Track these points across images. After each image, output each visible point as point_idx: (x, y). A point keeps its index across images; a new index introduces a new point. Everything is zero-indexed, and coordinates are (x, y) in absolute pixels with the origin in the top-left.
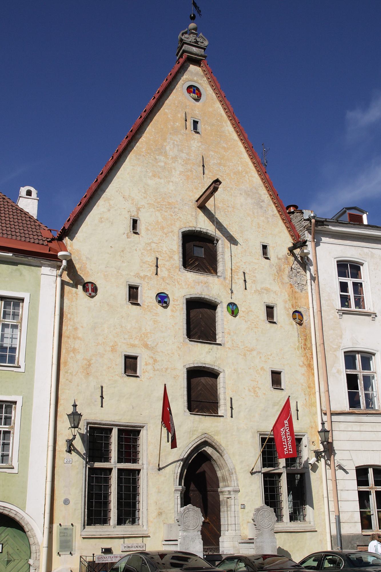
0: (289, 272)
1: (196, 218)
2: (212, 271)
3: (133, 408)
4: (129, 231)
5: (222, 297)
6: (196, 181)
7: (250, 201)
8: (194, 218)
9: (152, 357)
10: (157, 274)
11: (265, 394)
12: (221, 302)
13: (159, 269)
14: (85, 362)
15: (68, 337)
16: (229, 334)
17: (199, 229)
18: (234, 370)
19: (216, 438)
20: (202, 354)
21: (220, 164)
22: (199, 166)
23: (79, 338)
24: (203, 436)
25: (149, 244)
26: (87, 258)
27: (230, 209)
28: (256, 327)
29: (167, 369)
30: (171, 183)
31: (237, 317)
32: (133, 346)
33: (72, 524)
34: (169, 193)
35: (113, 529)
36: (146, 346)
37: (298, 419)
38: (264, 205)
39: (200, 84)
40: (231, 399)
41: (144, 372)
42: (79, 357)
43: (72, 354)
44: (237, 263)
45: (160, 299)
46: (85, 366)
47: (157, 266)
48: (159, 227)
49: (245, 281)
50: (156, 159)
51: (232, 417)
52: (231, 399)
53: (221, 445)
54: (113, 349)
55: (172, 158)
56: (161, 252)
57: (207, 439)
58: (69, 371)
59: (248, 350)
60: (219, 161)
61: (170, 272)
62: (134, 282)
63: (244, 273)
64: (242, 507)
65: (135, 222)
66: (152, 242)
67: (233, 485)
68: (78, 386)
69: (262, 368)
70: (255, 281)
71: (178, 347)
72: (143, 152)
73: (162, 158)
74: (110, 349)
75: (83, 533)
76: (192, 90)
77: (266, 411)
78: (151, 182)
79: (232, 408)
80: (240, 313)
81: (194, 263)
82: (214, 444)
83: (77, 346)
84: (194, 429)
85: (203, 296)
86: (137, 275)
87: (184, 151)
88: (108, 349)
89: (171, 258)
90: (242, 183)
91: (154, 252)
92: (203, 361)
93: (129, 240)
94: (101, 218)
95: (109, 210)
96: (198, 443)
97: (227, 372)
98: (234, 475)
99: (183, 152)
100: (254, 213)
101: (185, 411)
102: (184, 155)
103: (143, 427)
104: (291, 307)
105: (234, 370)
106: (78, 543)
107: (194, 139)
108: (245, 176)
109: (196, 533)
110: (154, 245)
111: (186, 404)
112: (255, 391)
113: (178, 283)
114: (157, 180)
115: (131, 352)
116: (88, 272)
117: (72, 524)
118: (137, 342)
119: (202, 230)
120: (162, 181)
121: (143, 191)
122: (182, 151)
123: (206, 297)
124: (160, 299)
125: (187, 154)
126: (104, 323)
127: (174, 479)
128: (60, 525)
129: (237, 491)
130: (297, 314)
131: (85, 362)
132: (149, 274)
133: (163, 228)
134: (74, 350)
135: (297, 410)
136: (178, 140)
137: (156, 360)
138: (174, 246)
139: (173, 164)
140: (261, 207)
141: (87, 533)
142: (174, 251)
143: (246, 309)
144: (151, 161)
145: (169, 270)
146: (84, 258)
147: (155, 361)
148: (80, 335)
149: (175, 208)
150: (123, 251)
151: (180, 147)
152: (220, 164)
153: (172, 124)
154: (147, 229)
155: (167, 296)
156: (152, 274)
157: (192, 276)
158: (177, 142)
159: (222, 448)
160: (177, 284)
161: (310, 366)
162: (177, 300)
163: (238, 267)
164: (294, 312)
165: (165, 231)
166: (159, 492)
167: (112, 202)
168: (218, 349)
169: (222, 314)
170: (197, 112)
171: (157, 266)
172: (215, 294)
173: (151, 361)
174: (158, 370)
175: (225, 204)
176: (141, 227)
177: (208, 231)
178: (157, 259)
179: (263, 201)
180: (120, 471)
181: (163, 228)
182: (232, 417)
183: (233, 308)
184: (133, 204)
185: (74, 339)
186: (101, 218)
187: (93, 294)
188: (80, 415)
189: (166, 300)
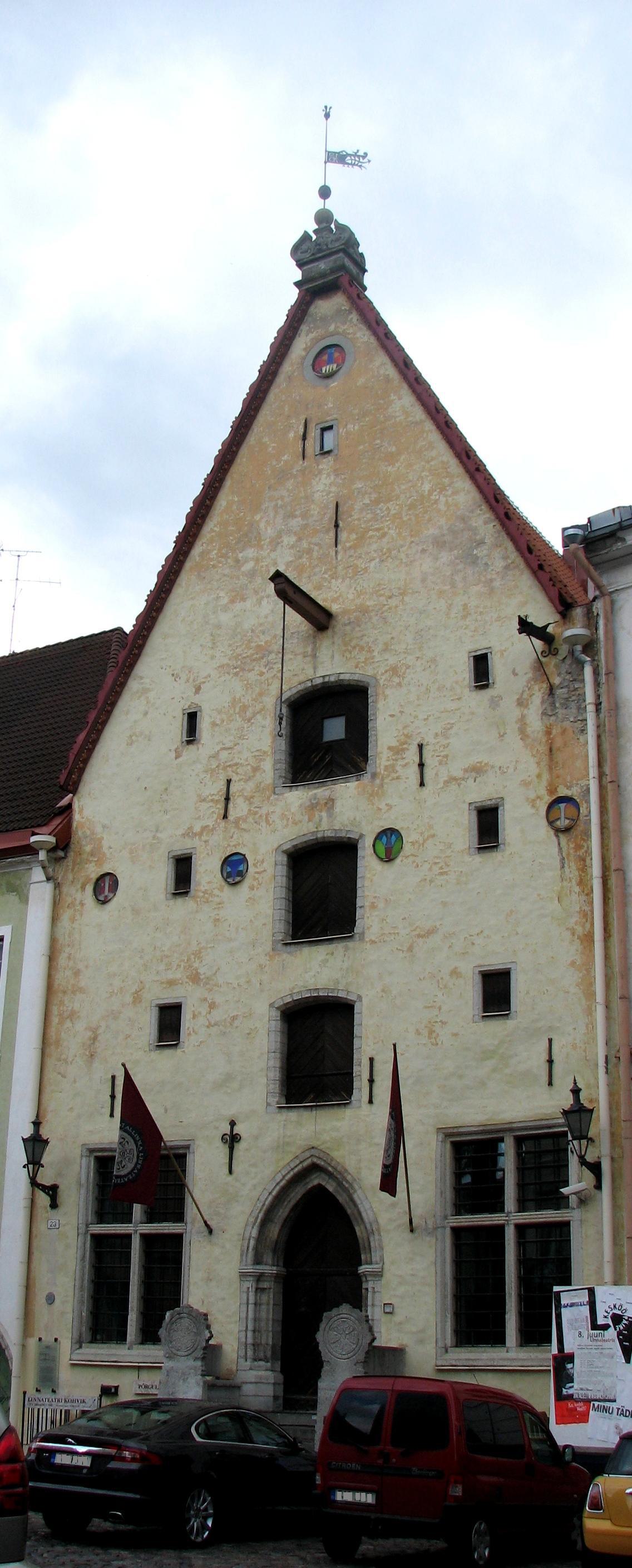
0: (543, 702)
1: (314, 656)
2: (353, 770)
3: (166, 1111)
4: (179, 743)
5: (363, 823)
6: (317, 570)
7: (445, 557)
8: (309, 659)
9: (205, 999)
10: (225, 817)
11: (456, 1035)
12: (362, 836)
13: (231, 805)
14: (89, 1034)
15: (65, 992)
16: (373, 906)
17: (319, 681)
18: (383, 991)
19: (335, 1154)
20: (316, 969)
21: (377, 502)
22: (327, 531)
23: (82, 990)
24: (308, 1154)
25: (215, 756)
26: (104, 827)
27: (393, 602)
28: (441, 874)
29: (234, 1018)
30: (264, 602)
31: (398, 861)
32: (171, 983)
33: (56, 1340)
34: (261, 625)
35: (127, 1352)
36: (195, 978)
37: (550, 1084)
38: (480, 552)
39: (332, 335)
40: (371, 1060)
41: (189, 1034)
42: (80, 1026)
43: (68, 1024)
44: (405, 727)
45: (229, 870)
46: (89, 1042)
47: (227, 799)
48: (237, 710)
49: (421, 765)
50: (237, 561)
51: (371, 1102)
52: (371, 1060)
53: (346, 1170)
54: (137, 998)
55: (271, 542)
56: (236, 764)
57: (315, 1160)
58: (64, 1056)
59: (419, 936)
60: (374, 496)
61: (251, 803)
62: (181, 847)
63: (421, 747)
64: (387, 1310)
65: (192, 718)
66: (222, 749)
67: (374, 1260)
68: (75, 1081)
69: (455, 973)
70: (446, 756)
71: (260, 966)
72: (212, 560)
73: (250, 552)
74: (131, 999)
75: (74, 1357)
76: (325, 357)
77: (461, 1077)
78: (224, 618)
79: (371, 1081)
80: (407, 848)
81: (322, 759)
82: (330, 1169)
83: (76, 1006)
84: (287, 1140)
85: (319, 835)
86: (189, 833)
87: (298, 513)
88: (128, 999)
89: (255, 769)
90: (430, 520)
91: (225, 768)
92: (312, 984)
93: (180, 759)
94: (131, 736)
95: (146, 714)
96: (296, 1170)
97: (365, 1001)
98: (377, 1237)
99: (294, 516)
100: (453, 585)
101: (268, 1104)
102: (295, 523)
103: (188, 1147)
104: (543, 791)
105: (383, 991)
106: (65, 1374)
107: (320, 472)
108: (436, 502)
109: (191, 1363)
110: (224, 755)
111: (276, 1087)
112: (431, 1032)
113: (267, 821)
114: (238, 606)
115: (169, 998)
116: (104, 854)
117: (56, 1340)
118: (178, 976)
119: (327, 679)
120: (248, 604)
121: (210, 645)
122: (292, 516)
123: (328, 834)
124: (229, 870)
125: (305, 516)
126: (129, 945)
127: (242, 1251)
128: (40, 1339)
129: (379, 1275)
130: (562, 806)
131: (89, 1034)
132: (210, 823)
133: (244, 708)
134: (73, 1015)
135: (550, 1062)
136: (285, 493)
137: (214, 1003)
138: (263, 742)
139: (273, 555)
140: (474, 561)
141: (80, 1358)
142: (265, 752)
143: (422, 834)
144: (227, 571)
145: (249, 799)
146: (99, 829)
147: (212, 1006)
148: (82, 984)
149: (270, 653)
150: (166, 789)
151: (289, 508)
152: (377, 502)
153: (274, 463)
154: (214, 724)
155: (244, 859)
156: (216, 821)
157: (298, 797)
158: (282, 498)
159: (349, 1178)
160: (264, 824)
161: (588, 939)
162: (263, 861)
163: (407, 736)
164: (551, 806)
165: (249, 714)
166: (209, 1280)
167: (151, 695)
168: (346, 949)
169: (368, 864)
170: (330, 405)
171: (227, 799)
172: (346, 822)
173: (204, 1009)
174: (216, 1024)
175: (381, 595)
176: (204, 725)
177: (342, 677)
178: (229, 782)
179: (481, 543)
180: (144, 1237)
181: (244, 708)
182: (371, 1102)
183: (388, 842)
184: (188, 681)
185: (74, 992)
186: (131, 736)
187: (111, 895)
188: (46, 1142)
189: (241, 868)
